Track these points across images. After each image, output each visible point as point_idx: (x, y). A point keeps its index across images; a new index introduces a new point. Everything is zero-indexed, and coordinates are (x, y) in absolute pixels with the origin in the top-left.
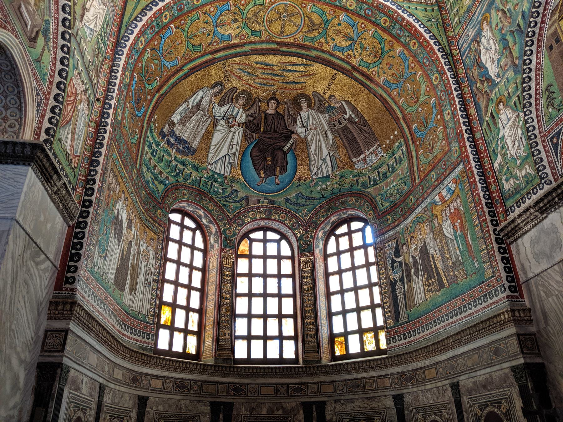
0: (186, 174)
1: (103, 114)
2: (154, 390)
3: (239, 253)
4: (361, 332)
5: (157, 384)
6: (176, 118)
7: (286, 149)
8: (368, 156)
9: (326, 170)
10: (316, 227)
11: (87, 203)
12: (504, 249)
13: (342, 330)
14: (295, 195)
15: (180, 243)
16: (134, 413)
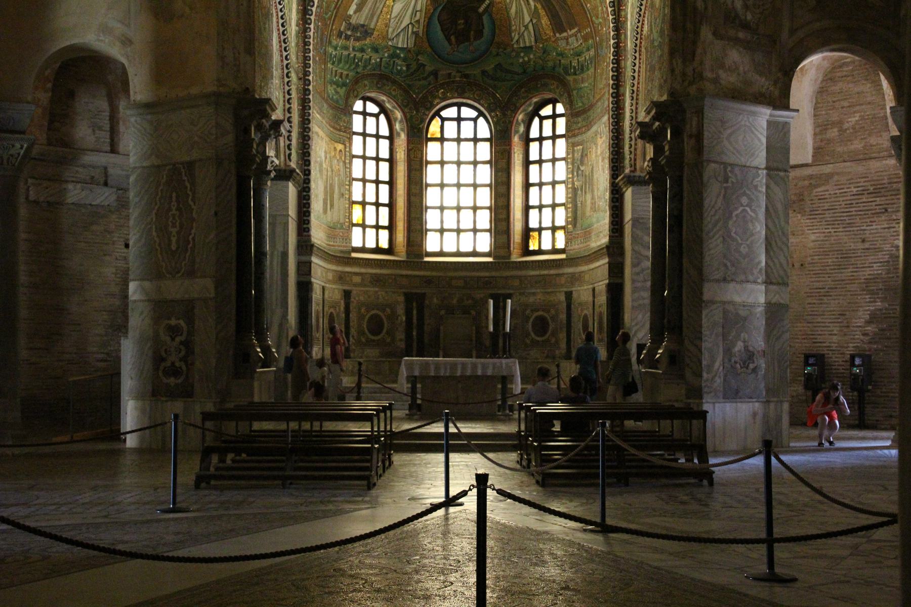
0: (366, 61)
1: (306, 92)
2: (355, 285)
3: (429, 136)
4: (554, 229)
5: (357, 279)
6: (351, 12)
7: (481, 10)
8: (571, 36)
9: (529, 40)
10: (515, 111)
11: (307, 173)
12: (617, 199)
13: (536, 226)
14: (493, 66)
15: (364, 135)
16: (342, 302)
